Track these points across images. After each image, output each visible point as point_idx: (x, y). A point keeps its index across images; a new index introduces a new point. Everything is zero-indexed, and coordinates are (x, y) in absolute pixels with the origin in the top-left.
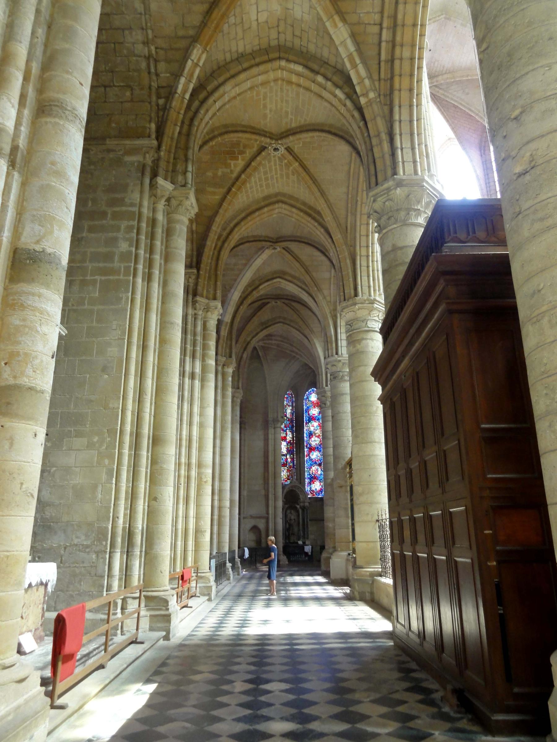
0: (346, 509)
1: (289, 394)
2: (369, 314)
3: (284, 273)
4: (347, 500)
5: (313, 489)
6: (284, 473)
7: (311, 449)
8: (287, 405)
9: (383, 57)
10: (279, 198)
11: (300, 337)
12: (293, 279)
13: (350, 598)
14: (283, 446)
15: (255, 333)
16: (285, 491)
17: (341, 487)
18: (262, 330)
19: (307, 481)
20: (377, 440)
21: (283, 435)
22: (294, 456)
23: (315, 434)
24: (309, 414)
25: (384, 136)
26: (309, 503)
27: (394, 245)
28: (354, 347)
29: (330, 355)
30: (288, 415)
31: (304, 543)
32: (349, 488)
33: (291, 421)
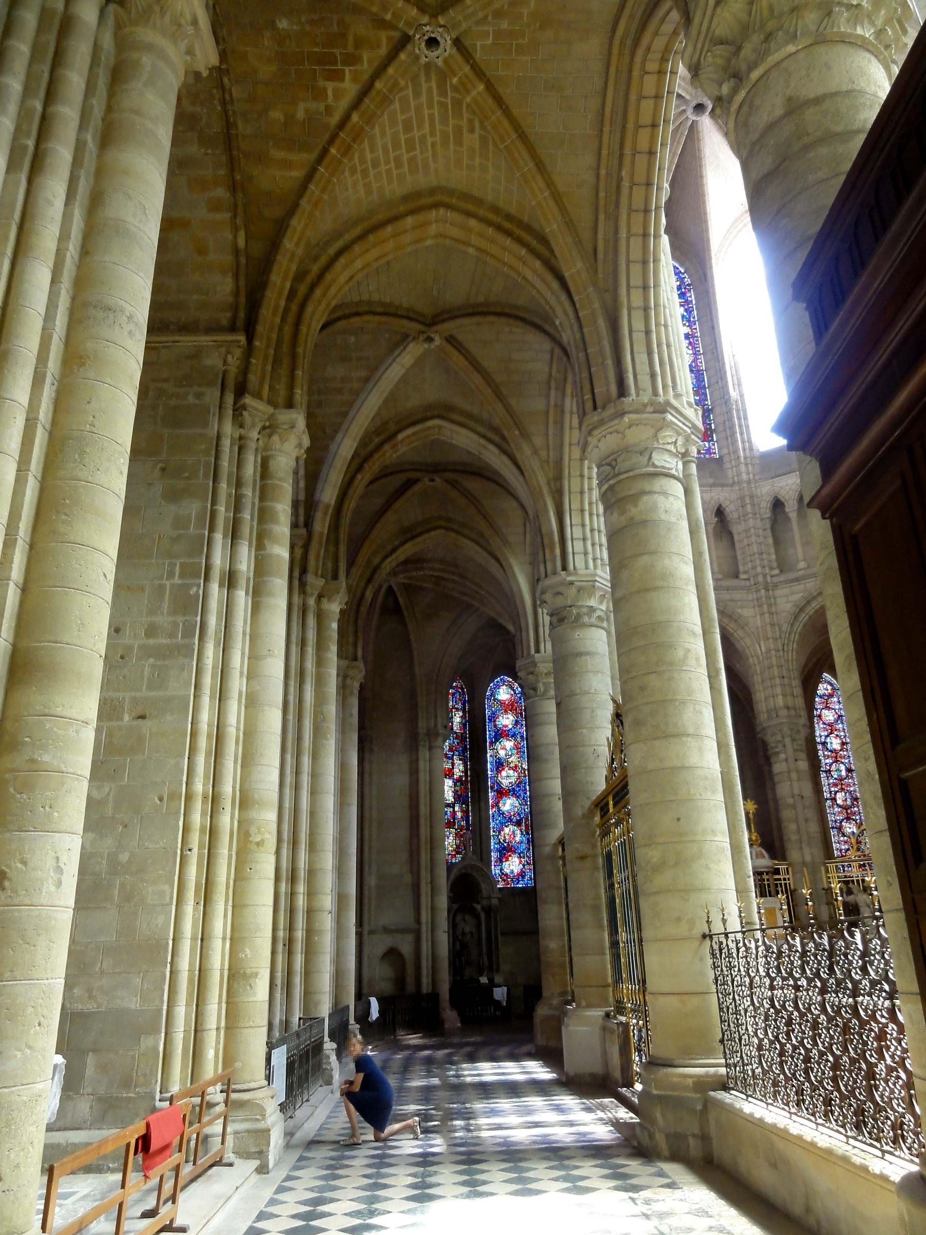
0: (596, 909)
1: (456, 687)
3: (450, 408)
4: (597, 886)
5: (507, 871)
6: (450, 842)
7: (501, 793)
8: (454, 707)
10: (438, 197)
11: (480, 556)
12: (468, 420)
14: (446, 788)
15: (389, 548)
16: (452, 877)
17: (583, 858)
19: (494, 855)
20: (691, 731)
22: (468, 806)
23: (509, 764)
24: (495, 726)
26: (498, 898)
27: (789, 99)
28: (623, 512)
29: (549, 572)
30: (456, 728)
31: (491, 980)
32: (600, 861)
33: (461, 738)
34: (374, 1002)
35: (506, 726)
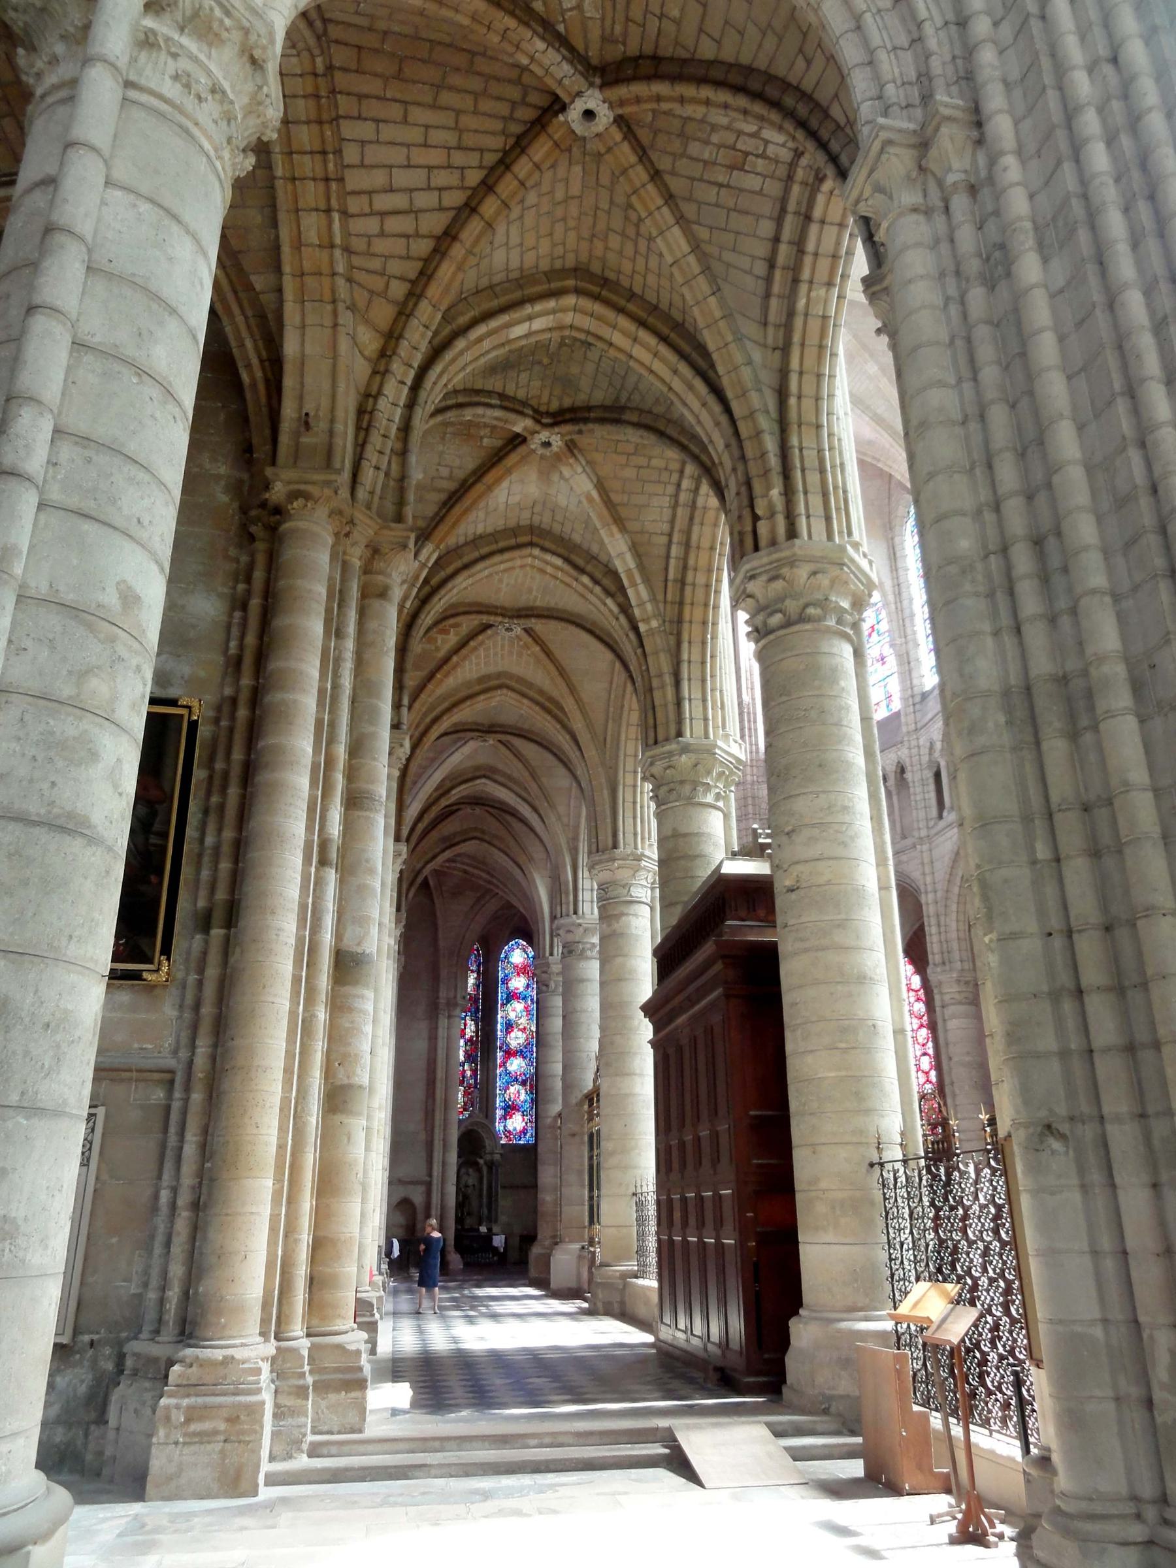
0: (581, 1172)
2: (634, 876)
3: (494, 770)
4: (582, 1157)
5: (510, 1128)
7: (509, 1054)
9: (671, 576)
11: (510, 865)
12: (508, 782)
13: (591, 1313)
15: (430, 855)
17: (573, 1135)
18: (443, 851)
19: (499, 1113)
20: (638, 1072)
23: (518, 1025)
24: (507, 988)
25: (668, 679)
27: (674, 830)
28: (609, 925)
31: (490, 1230)
32: (586, 1138)
34: (395, 1241)
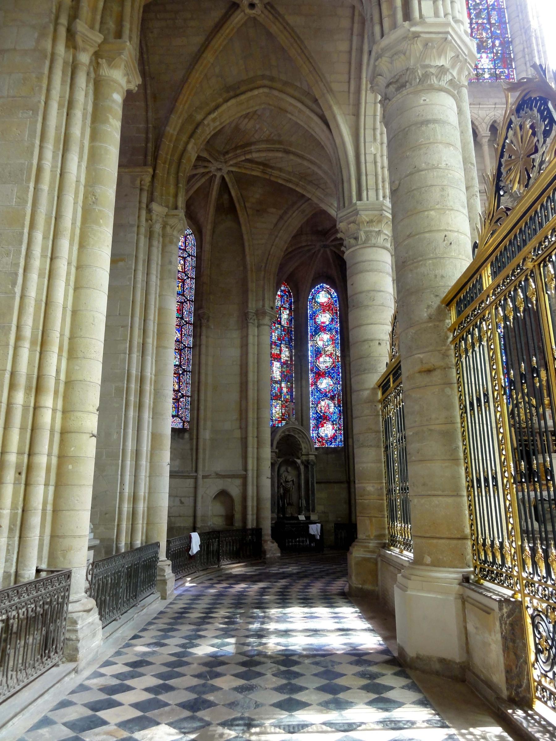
1: (284, 290)
6: (277, 410)
7: (319, 375)
8: (282, 306)
14: (274, 369)
15: (213, 104)
16: (277, 437)
18: (226, 101)
19: (312, 423)
21: (275, 351)
22: (292, 383)
24: (315, 323)
26: (315, 455)
30: (284, 322)
31: (308, 518)
33: (288, 331)
35: (323, 323)
